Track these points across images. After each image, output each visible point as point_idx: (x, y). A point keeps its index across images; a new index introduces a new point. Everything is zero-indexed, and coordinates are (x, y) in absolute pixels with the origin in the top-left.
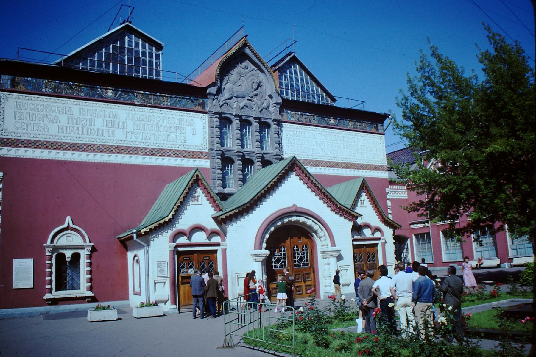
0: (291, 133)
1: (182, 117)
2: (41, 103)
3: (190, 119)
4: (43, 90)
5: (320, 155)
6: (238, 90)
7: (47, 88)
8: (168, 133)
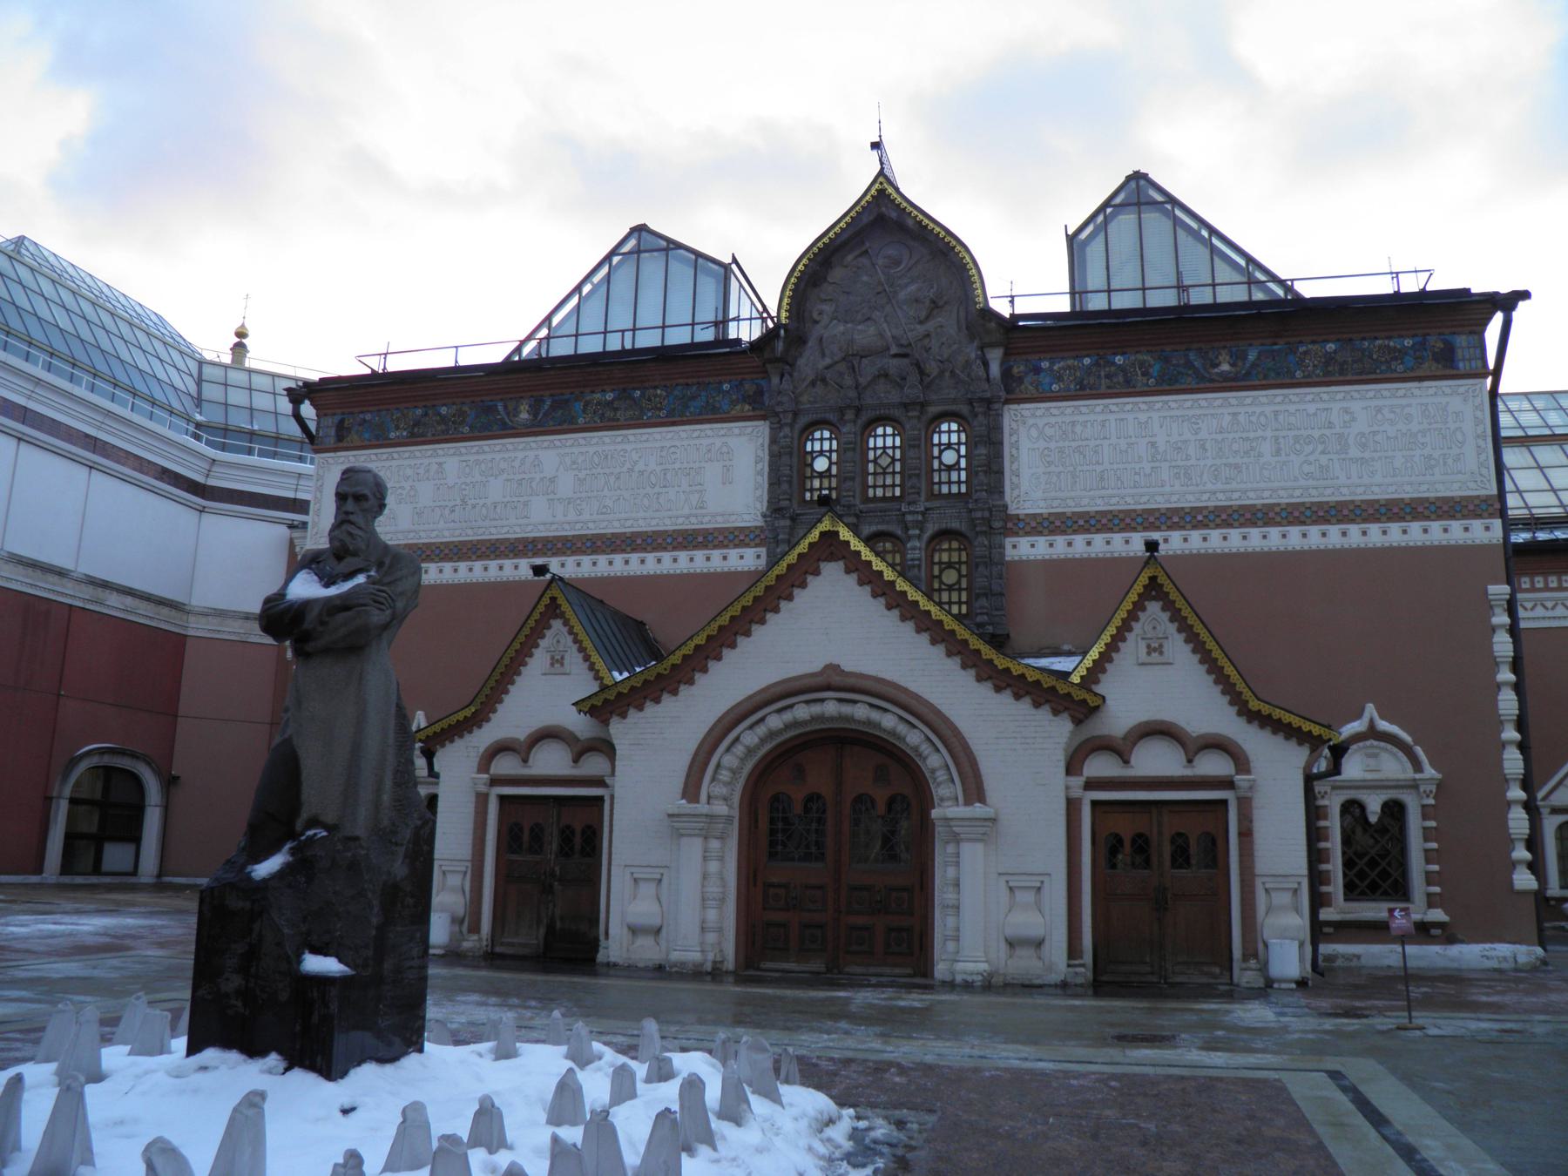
0: (1049, 431)
1: (697, 442)
2: (387, 464)
3: (718, 442)
4: (392, 435)
5: (1167, 489)
6: (865, 335)
7: (397, 428)
8: (657, 489)
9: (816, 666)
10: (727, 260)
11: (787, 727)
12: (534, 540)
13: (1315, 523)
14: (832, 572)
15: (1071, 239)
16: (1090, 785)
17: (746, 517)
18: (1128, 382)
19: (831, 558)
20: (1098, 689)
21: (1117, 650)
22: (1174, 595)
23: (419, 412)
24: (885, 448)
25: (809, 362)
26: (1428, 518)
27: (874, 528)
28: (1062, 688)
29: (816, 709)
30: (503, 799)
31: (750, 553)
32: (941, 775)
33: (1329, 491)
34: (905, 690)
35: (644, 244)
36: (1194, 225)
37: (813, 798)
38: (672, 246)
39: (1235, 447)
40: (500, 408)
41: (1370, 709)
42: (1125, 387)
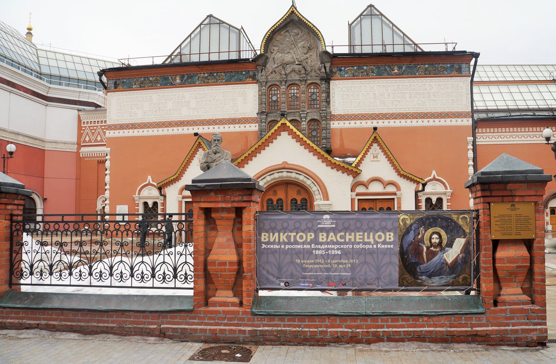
2: (132, 96)
4: (134, 87)
6: (288, 58)
7: (135, 84)
8: (223, 105)
9: (281, 163)
10: (240, 28)
11: (272, 180)
12: (183, 121)
13: (420, 118)
14: (284, 134)
15: (350, 25)
16: (357, 195)
17: (252, 114)
18: (367, 74)
19: (284, 131)
20: (359, 168)
21: (365, 157)
22: (381, 142)
23: (142, 79)
24: (294, 93)
25: (271, 66)
26: (452, 118)
27: (291, 118)
28: (350, 168)
29: (280, 174)
30: (186, 202)
31: (253, 125)
32: (317, 192)
33: (425, 109)
34: (306, 169)
35: (211, 20)
37: (278, 200)
38: (221, 22)
39: (398, 95)
40: (170, 78)
41: (434, 172)
42: (367, 76)
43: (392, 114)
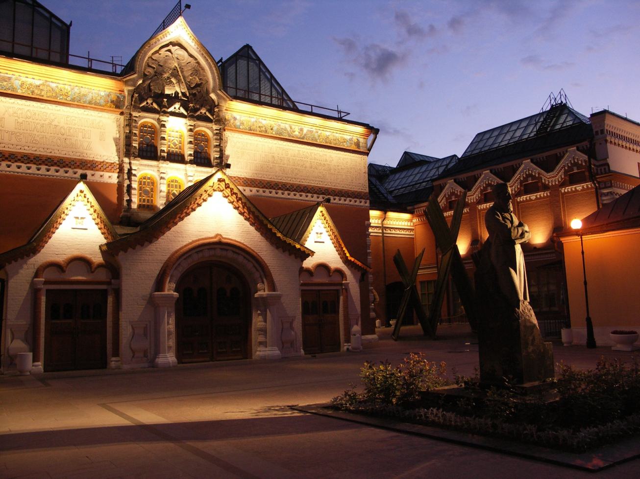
10: (68, 23)
30: (48, 291)
36: (264, 70)
43: (292, 185)
